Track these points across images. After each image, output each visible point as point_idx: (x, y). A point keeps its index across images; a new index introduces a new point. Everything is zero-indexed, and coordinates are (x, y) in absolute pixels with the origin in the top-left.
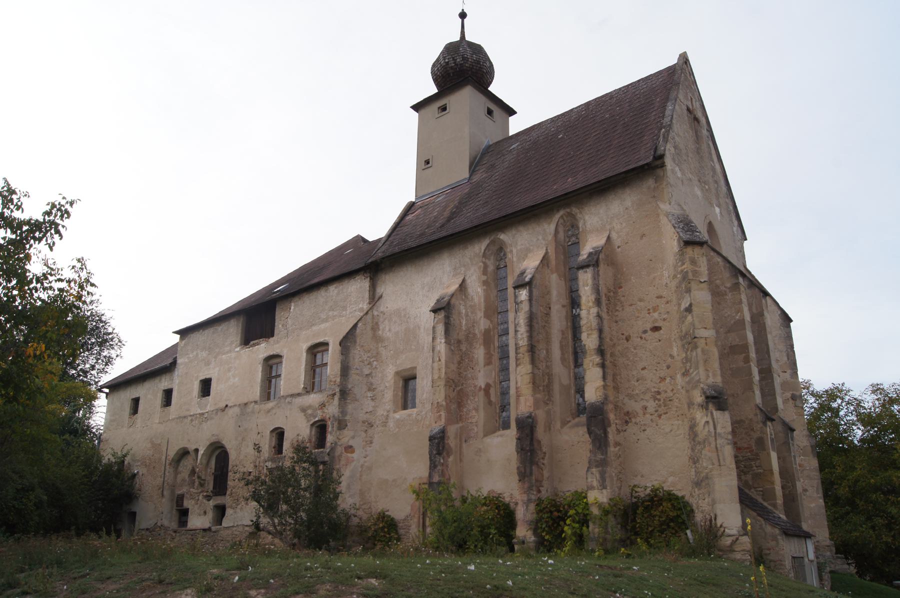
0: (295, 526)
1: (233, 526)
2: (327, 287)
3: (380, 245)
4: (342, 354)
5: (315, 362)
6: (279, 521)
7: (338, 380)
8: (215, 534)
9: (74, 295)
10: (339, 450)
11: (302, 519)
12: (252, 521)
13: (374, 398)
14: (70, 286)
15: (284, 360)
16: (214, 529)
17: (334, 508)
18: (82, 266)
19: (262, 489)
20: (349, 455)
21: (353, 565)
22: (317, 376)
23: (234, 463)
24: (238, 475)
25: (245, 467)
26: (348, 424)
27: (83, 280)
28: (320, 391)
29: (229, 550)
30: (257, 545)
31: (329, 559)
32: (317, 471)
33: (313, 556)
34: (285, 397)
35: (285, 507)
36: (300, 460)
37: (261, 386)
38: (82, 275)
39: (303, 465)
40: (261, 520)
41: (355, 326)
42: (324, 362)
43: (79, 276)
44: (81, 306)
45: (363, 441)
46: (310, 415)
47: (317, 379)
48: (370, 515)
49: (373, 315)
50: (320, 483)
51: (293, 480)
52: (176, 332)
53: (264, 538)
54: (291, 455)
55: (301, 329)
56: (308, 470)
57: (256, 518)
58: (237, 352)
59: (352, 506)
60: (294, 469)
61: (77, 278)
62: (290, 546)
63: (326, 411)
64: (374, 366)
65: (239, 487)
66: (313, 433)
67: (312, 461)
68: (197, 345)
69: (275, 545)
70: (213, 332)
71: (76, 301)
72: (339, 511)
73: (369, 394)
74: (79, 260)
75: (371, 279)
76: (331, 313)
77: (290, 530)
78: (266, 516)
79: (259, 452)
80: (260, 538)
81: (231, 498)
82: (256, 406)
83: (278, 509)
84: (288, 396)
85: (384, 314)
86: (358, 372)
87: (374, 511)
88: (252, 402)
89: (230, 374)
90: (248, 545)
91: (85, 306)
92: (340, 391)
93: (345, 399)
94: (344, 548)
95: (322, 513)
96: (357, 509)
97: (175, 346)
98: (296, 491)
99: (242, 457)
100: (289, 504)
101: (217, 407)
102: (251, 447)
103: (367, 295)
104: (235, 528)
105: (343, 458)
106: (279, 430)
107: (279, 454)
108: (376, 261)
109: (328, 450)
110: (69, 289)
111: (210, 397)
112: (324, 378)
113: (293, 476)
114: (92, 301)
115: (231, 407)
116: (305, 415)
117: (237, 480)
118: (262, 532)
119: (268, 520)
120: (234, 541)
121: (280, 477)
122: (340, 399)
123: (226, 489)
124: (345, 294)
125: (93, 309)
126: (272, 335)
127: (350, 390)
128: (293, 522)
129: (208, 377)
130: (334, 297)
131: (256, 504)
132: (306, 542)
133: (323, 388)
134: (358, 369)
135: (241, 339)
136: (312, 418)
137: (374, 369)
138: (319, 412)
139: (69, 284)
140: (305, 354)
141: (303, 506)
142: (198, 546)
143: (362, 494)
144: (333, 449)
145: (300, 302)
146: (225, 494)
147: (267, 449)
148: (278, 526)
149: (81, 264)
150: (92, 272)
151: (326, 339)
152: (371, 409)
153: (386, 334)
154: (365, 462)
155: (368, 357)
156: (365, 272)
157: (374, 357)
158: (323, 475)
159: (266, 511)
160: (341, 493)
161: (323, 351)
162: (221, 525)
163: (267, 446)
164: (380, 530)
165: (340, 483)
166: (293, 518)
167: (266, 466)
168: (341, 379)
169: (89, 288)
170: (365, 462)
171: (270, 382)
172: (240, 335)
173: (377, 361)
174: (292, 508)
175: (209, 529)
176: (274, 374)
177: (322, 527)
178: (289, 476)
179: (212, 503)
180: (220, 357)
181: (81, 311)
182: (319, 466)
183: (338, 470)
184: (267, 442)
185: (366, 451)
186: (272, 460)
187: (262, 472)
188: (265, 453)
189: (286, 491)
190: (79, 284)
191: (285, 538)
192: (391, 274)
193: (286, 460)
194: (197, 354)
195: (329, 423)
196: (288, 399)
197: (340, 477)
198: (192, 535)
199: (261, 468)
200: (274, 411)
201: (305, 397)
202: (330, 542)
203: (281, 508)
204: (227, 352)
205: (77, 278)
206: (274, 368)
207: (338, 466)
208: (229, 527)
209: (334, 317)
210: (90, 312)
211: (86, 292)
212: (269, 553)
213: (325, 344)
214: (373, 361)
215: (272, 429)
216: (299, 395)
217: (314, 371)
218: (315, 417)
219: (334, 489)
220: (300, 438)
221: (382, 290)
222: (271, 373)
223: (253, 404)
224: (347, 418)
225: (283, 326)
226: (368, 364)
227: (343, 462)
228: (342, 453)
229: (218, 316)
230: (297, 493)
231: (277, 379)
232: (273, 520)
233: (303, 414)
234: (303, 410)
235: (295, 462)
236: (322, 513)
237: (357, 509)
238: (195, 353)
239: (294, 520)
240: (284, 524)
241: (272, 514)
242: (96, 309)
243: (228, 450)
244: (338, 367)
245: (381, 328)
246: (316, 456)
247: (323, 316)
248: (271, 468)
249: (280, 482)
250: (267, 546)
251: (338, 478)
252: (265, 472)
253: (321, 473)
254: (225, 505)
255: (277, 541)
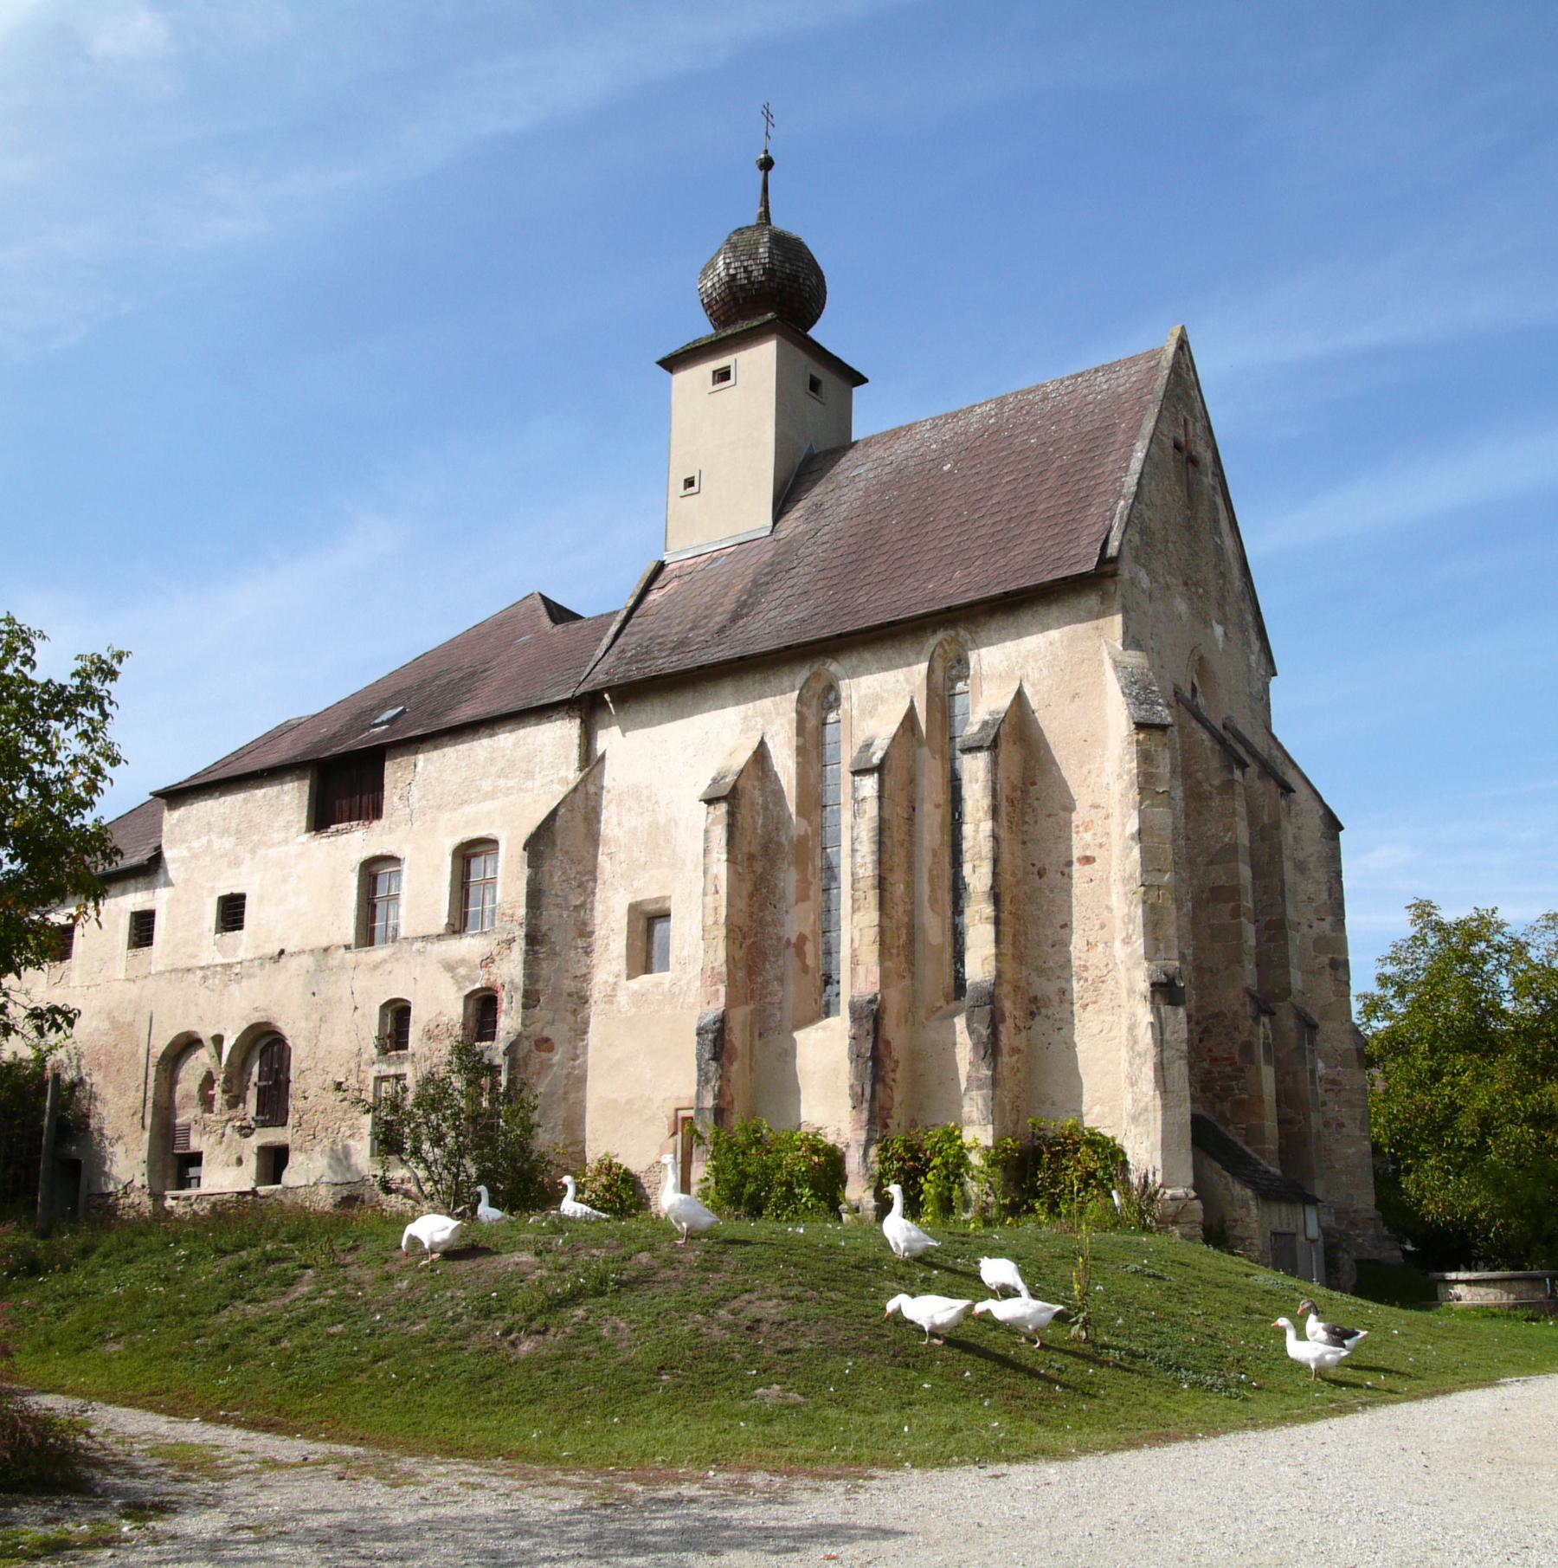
15: (405, 867)
20: (544, 1054)
23: (304, 1066)
41: (553, 814)
46: (463, 977)
55: (439, 807)
68: (209, 824)
73: (580, 943)
76: (502, 782)
84: (416, 938)
86: (559, 900)
88: (339, 947)
99: (321, 1053)
101: (260, 953)
106: (399, 1004)
127: (545, 935)
129: (237, 891)
135: (309, 817)
136: (467, 983)
140: (449, 859)
146: (284, 1124)
196: (418, 945)
200: (388, 967)
218: (474, 982)
223: (343, 950)
228: (530, 1051)
233: (450, 975)
234: (450, 967)
238: (204, 840)
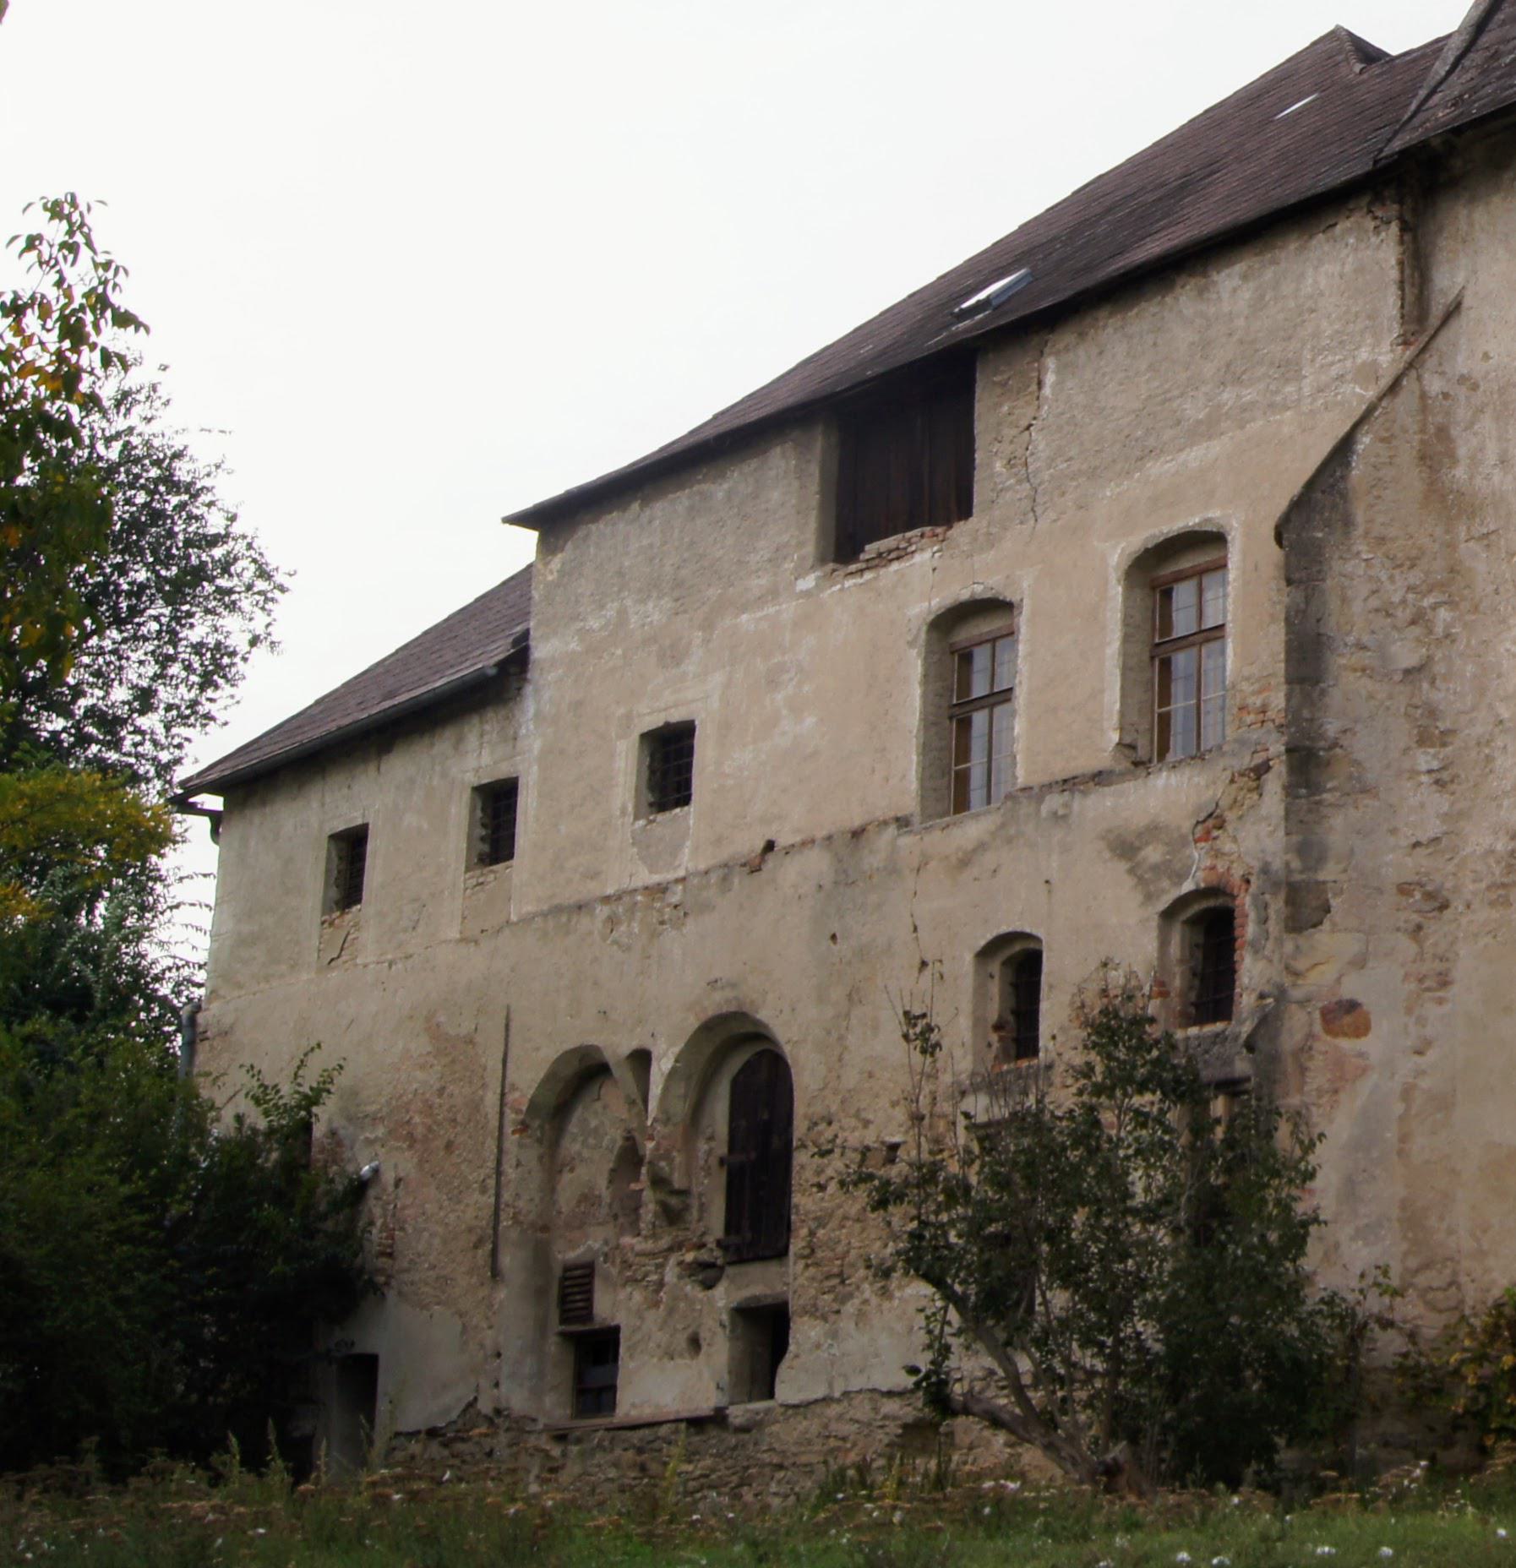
0: (1115, 1384)
1: (827, 1400)
2: (1205, 275)
3: (1441, 68)
4: (1289, 582)
5: (1166, 624)
6: (1037, 1364)
7: (1278, 700)
8: (746, 1436)
9: (39, 370)
10: (1297, 1025)
11: (1141, 1349)
12: (913, 1370)
13: (1445, 776)
14: (18, 330)
15: (1023, 622)
16: (738, 1414)
17: (1290, 1294)
18: (71, 233)
19: (952, 1223)
20: (1345, 1044)
21: (1387, 1551)
22: (1178, 689)
23: (818, 1109)
24: (836, 1165)
25: (866, 1123)
26: (1334, 902)
27: (78, 300)
28: (1199, 756)
29: (815, 1509)
30: (940, 1480)
31: (1274, 1531)
32: (1200, 1127)
33: (1204, 1519)
34: (1035, 793)
35: (1061, 1299)
36: (1120, 1081)
37: (925, 749)
38: (71, 275)
39: (1137, 1101)
40: (952, 1362)
41: (1343, 449)
42: (1209, 623)
43: (60, 283)
44: (76, 420)
45: (1406, 976)
46: (1155, 868)
47: (1180, 704)
48: (1453, 1318)
49: (1423, 396)
50: (1216, 1180)
51: (1091, 1171)
52: (522, 519)
53: (971, 1448)
54: (1078, 1059)
55: (1093, 474)
56: (1159, 1121)
57: (929, 1355)
58: (807, 594)
59: (1369, 1280)
60: (1096, 1123)
61: (52, 294)
62: (1092, 1477)
63: (1228, 846)
64: (1439, 630)
65: (845, 1218)
66: (1175, 949)
67: (1178, 1081)
68: (620, 574)
69: (1022, 1476)
70: (691, 508)
71: (54, 396)
72: (1310, 1304)
73: (1425, 760)
74: (55, 210)
75: (1405, 228)
76: (1228, 396)
77: (1088, 1404)
78: (978, 1346)
79: (930, 1049)
80: (953, 1445)
81: (812, 1270)
82: (906, 841)
83: (1030, 1310)
84: (1048, 787)
85: (1475, 387)
86: (1366, 658)
87: (1471, 1296)
88: (885, 823)
89: (780, 697)
90: (901, 1483)
91: (96, 416)
92: (1289, 751)
93: (1314, 788)
94: (1343, 1475)
95: (1234, 1320)
96: (1395, 1293)
97: (520, 583)
98: (1107, 1222)
99: (851, 1078)
100: (1077, 1287)
101: (724, 854)
102: (892, 1027)
103: (1390, 304)
104: (834, 1410)
105: (1317, 1063)
106: (1018, 947)
107: (1019, 1056)
108: (1423, 146)
109: (1246, 1029)
110: (17, 342)
111: (692, 809)
112: (1211, 694)
113: (1093, 1152)
114: (126, 394)
115: (788, 851)
116: (1131, 871)
117: (832, 1187)
118: (961, 1420)
119: (989, 1362)
120: (834, 1467)
121: (1030, 1164)
122: (1290, 790)
123: (784, 1227)
124: (1292, 304)
125: (131, 430)
126: (964, 509)
127: (1335, 744)
128: (1100, 1366)
129: (676, 716)
130: (1241, 322)
131: (926, 1289)
132: (1165, 1454)
133: (1210, 739)
134: (1364, 648)
135: (822, 532)
136: (1165, 883)
137: (1439, 641)
138: (1198, 856)
139: (18, 321)
140: (1117, 591)
141: (1144, 1290)
142: (671, 1498)
143: (1412, 1220)
144: (1268, 1021)
145: (1081, 351)
146: (781, 1254)
147: (967, 1036)
148: (1035, 1386)
149: (64, 225)
150: (119, 261)
151: (1215, 513)
152: (1434, 828)
153: (1488, 477)
154: (1420, 1073)
155: (1410, 589)
156: (1378, 199)
157: (1441, 586)
158: (1230, 1143)
159: (978, 1321)
160: (1316, 1220)
161: (1200, 573)
162: (771, 1395)
163: (964, 1023)
164: (1504, 1386)
165: (1310, 1175)
166: (1102, 1345)
167: (967, 1115)
168: (1289, 697)
169: (110, 337)
170: (1420, 1073)
171: (965, 725)
172: (814, 514)
173: (1451, 604)
174: (1095, 1300)
175: (718, 1418)
176: (979, 689)
177: (1238, 1384)
178: (1074, 1155)
179: (724, 1297)
180: (728, 621)
181: (78, 442)
182: (1207, 1102)
183: (1299, 1118)
184: (966, 1004)
185: (1421, 1021)
186: (992, 1085)
187: (949, 1142)
188: (958, 1053)
189: (1065, 1224)
190: (63, 319)
191: (1071, 1439)
192: (1496, 200)
193: (1057, 1080)
194: (622, 613)
195: (1246, 903)
196: (1054, 802)
197: (1309, 1148)
198: (640, 1451)
199: (942, 1126)
200: (989, 859)
201: (1129, 786)
202: (1273, 1448)
203: (1045, 1302)
204: (761, 601)
205: (52, 294)
206: (981, 658)
207: (1294, 1100)
208: (808, 1404)
209: (1243, 414)
210: (117, 446)
211: (97, 354)
212: (999, 1513)
213: (1213, 539)
214: (1434, 607)
215: (983, 943)
216: (1100, 778)
217: (1166, 665)
218: (1180, 877)
219: (1285, 1207)
220: (1117, 977)
221: (1460, 279)
222: (965, 684)
223: (892, 830)
224: (1329, 873)
225: (1010, 463)
226: (1413, 622)
227: (1318, 1078)
228: (1311, 1036)
229: (710, 433)
230: (1113, 1232)
231: (998, 710)
232: (1008, 1363)
233: (1123, 866)
234: (1125, 847)
235: (1098, 1090)
236: (1234, 1320)
237: (1395, 1293)
238: (611, 610)
239: (1108, 1358)
240: (1061, 1380)
241: (1002, 1336)
242: (147, 430)
243: (787, 1050)
244: (1274, 640)
245: (1462, 451)
246: (1190, 1059)
247: (1194, 410)
248: (989, 1124)
249: (1031, 1183)
250: (988, 1484)
251: (1298, 1153)
252: (961, 1141)
253: (1220, 1132)
254: (785, 1304)
255: (1031, 1456)
